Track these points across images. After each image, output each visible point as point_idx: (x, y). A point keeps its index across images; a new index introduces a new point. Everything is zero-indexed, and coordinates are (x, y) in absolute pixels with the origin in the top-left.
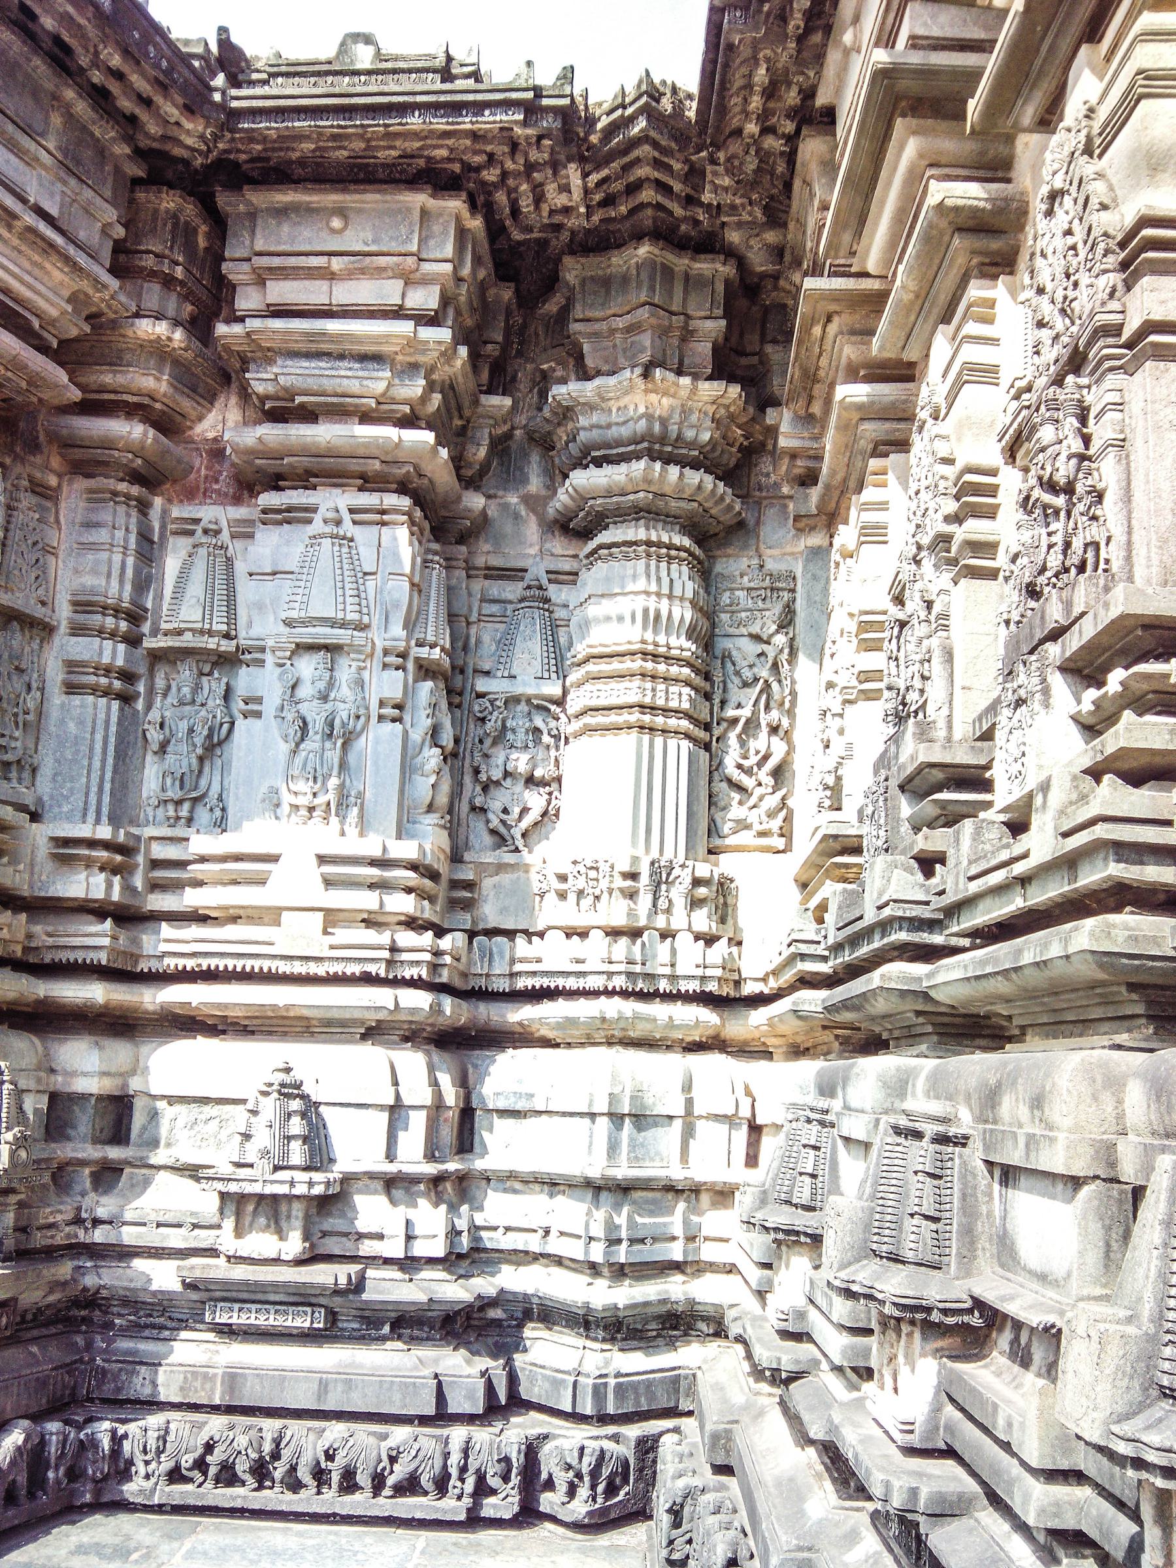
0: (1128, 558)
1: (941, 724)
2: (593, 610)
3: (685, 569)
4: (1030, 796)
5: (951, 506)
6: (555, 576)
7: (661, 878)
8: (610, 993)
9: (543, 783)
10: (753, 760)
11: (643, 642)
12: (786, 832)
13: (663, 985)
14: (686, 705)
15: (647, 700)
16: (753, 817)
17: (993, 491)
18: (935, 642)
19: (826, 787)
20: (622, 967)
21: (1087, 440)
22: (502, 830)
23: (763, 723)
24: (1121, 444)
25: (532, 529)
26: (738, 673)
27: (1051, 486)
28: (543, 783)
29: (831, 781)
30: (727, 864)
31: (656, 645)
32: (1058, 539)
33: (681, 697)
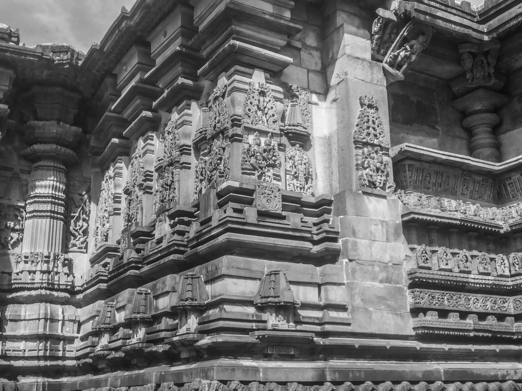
0: (179, 200)
1: (140, 223)
2: (37, 183)
3: (63, 175)
4: (163, 237)
5: (144, 178)
6: (23, 172)
7: (56, 258)
8: (41, 288)
9: (17, 230)
10: (78, 228)
11: (52, 194)
12: (86, 248)
13: (56, 286)
14: (62, 212)
15: (53, 210)
16: (77, 243)
17: (152, 176)
18: (139, 206)
19: (104, 236)
20: (46, 281)
21: (173, 178)
22: (5, 243)
23: (82, 218)
24: (179, 181)
25: (15, 157)
26: (75, 204)
27: (167, 185)
28: (17, 230)
29: (106, 234)
30: (70, 256)
31: (55, 195)
32: (168, 194)
33: (61, 210)
